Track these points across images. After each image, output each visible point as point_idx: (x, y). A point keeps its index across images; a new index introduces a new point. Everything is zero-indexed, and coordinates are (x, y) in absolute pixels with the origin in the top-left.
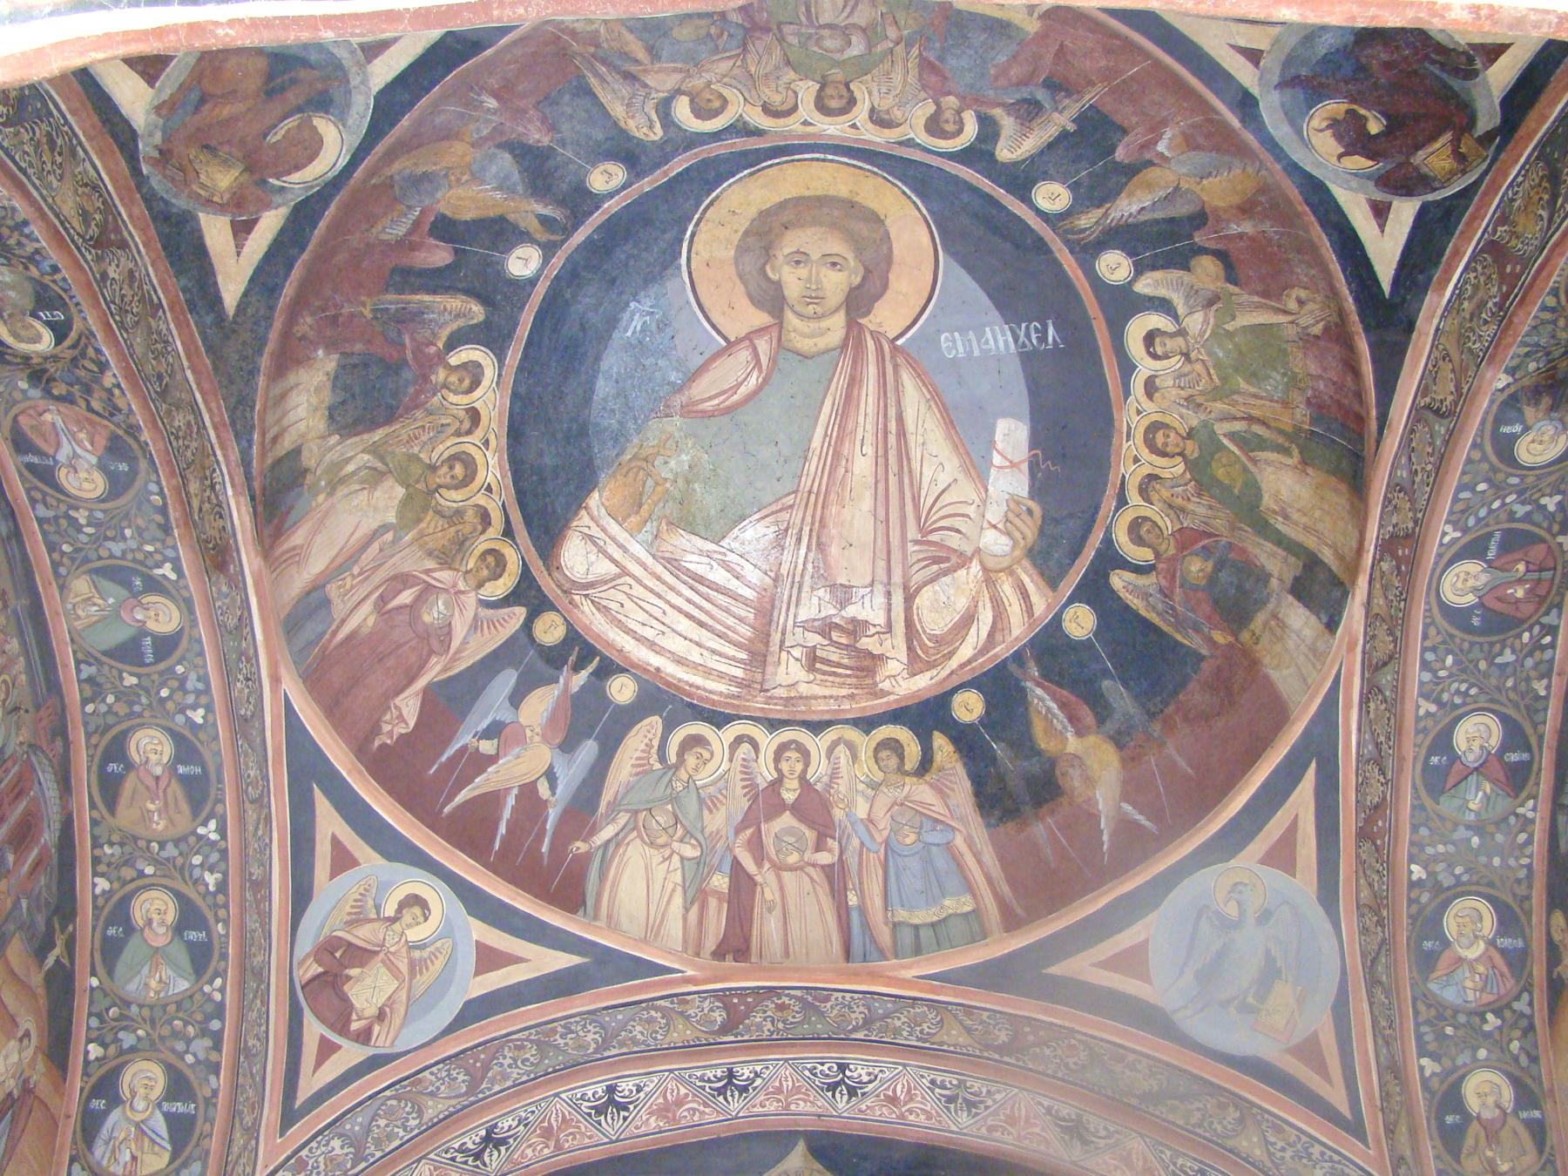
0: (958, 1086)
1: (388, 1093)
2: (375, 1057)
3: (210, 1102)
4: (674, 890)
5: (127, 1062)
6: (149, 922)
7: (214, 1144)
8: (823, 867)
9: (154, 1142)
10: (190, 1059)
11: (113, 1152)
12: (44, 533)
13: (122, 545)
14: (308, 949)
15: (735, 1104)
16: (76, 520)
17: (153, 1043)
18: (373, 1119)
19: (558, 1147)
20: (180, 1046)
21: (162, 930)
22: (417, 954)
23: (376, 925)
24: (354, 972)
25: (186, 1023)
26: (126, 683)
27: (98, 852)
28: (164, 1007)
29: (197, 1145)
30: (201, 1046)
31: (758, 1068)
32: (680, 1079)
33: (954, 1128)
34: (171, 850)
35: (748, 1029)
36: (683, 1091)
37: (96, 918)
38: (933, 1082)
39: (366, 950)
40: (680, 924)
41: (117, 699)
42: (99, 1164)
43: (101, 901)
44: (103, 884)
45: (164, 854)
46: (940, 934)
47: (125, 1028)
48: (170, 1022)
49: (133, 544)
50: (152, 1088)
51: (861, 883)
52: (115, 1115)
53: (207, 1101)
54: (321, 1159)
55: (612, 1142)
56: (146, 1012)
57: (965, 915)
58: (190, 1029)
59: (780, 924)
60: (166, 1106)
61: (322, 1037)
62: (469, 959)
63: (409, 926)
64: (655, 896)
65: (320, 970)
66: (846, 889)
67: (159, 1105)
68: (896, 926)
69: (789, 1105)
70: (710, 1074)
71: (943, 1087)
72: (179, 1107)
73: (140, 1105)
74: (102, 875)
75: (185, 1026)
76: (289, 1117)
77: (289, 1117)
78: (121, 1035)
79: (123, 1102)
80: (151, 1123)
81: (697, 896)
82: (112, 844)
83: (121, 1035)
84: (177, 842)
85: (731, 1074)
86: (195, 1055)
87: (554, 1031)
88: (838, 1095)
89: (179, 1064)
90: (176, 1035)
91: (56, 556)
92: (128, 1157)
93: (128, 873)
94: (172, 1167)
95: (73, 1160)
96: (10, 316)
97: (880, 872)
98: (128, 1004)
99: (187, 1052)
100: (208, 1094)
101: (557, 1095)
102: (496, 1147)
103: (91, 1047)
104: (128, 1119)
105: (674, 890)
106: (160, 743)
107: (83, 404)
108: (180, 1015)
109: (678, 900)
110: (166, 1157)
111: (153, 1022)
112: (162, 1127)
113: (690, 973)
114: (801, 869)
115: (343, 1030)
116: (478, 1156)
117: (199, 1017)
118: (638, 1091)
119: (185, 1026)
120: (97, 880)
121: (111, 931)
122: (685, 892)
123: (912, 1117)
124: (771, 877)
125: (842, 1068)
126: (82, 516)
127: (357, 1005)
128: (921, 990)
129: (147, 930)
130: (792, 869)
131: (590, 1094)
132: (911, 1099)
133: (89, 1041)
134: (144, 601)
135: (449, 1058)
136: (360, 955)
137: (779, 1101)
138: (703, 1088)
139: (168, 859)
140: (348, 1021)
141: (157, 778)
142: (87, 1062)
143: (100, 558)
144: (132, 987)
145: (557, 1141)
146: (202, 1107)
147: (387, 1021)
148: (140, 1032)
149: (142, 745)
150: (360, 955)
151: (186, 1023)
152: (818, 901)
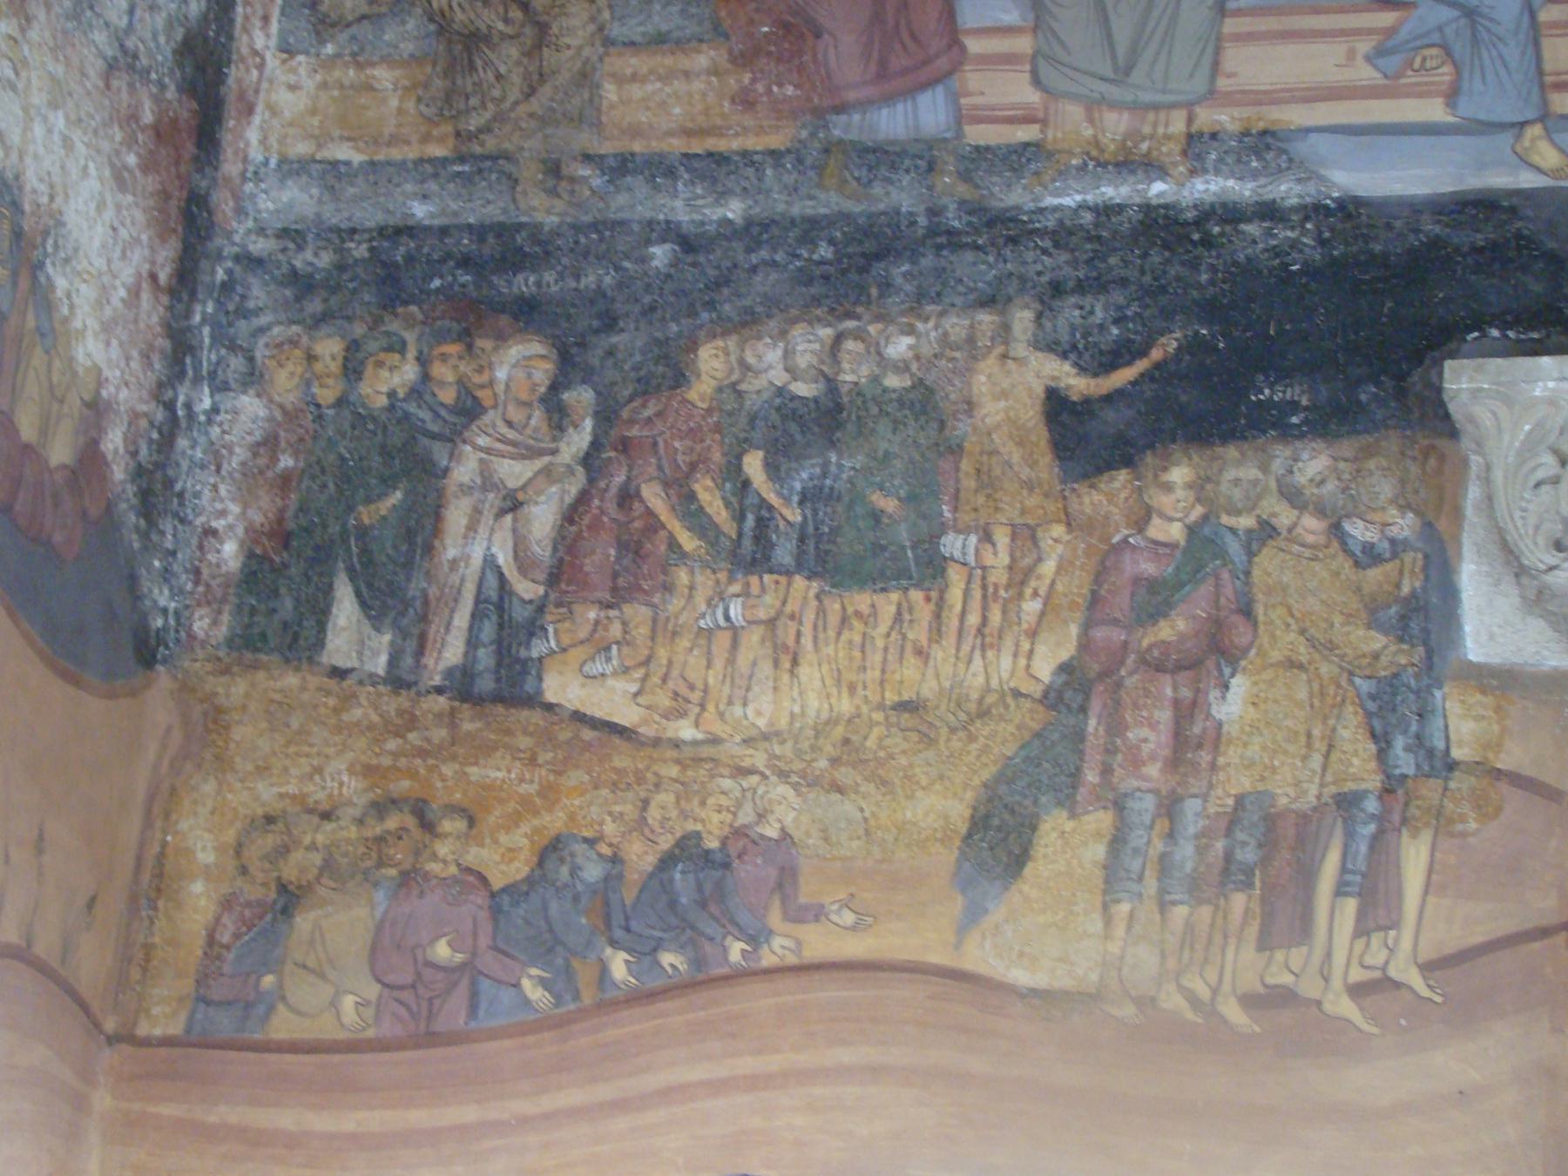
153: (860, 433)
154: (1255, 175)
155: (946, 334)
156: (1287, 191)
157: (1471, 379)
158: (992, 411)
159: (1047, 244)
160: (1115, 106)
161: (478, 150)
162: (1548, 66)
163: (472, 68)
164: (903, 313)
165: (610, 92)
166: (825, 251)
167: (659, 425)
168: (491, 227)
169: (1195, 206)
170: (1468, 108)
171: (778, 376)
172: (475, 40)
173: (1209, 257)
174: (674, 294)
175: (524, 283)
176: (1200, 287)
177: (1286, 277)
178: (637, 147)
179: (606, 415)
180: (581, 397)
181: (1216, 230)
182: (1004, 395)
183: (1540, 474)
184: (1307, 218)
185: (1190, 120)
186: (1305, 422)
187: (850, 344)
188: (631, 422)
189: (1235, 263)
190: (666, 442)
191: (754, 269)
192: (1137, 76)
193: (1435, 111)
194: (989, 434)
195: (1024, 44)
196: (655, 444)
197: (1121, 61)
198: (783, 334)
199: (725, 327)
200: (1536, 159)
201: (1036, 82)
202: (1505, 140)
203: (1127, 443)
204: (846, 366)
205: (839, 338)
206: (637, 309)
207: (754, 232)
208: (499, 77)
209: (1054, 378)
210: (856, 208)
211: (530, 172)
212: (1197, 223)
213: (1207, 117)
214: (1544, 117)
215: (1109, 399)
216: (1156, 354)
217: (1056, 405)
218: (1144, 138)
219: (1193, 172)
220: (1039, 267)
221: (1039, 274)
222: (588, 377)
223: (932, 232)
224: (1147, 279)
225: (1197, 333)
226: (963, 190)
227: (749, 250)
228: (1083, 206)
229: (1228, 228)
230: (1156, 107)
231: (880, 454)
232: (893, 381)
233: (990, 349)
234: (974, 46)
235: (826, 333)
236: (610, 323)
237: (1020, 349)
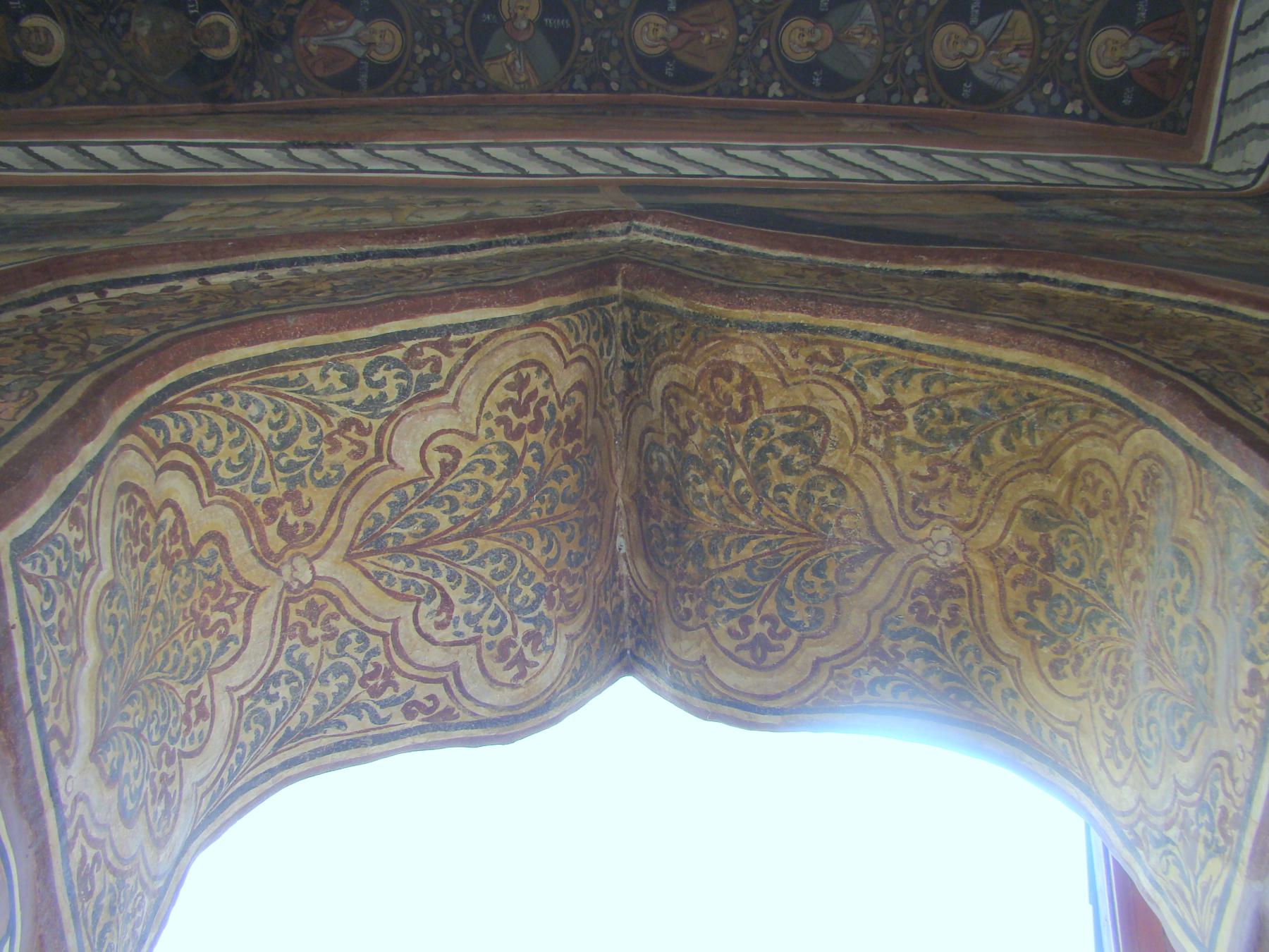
6: (810, 45)
9: (1004, 28)
11: (1009, 70)
12: (442, 92)
13: (450, 22)
16: (426, 58)
21: (818, 32)
26: (591, 49)
27: (745, 92)
34: (746, 22)
37: (804, 97)
41: (606, 60)
43: (790, 91)
44: (775, 89)
45: (750, 29)
47: (904, 66)
49: (447, 12)
50: (957, 37)
52: (979, 73)
56: (890, 48)
60: (974, 21)
67: (973, 27)
73: (971, 47)
74: (767, 89)
78: (909, 70)
79: (968, 65)
82: (739, 79)
83: (909, 70)
84: (739, 17)
91: (465, 87)
92: (1015, 55)
93: (765, 65)
95: (1012, 110)
96: (196, 38)
98: (882, 66)
103: (916, 100)
106: (647, 24)
107: (292, 12)
120: (770, 94)
121: (817, 81)
126: (421, 54)
129: (818, 48)
133: (911, 103)
134: (507, 16)
139: (754, 26)
141: (681, 31)
142: (930, 104)
143: (464, 46)
144: (867, 62)
148: (908, 53)
149: (649, 43)
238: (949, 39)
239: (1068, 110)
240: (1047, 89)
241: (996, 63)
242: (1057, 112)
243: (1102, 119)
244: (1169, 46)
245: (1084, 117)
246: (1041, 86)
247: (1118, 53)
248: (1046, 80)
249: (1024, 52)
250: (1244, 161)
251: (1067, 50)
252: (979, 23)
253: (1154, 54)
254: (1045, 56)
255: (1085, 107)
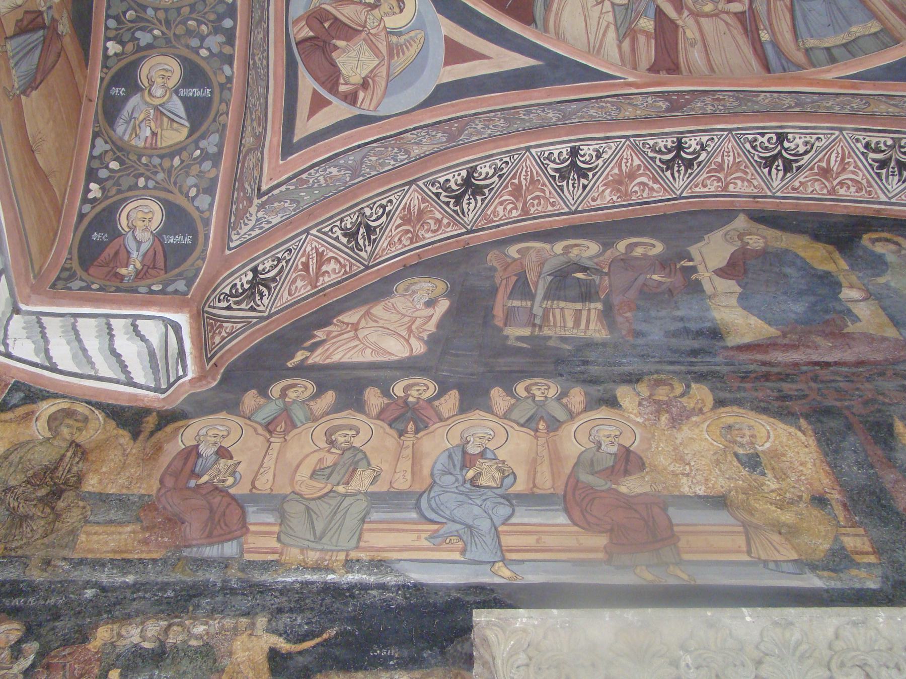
0: (892, 147)
1: (374, 145)
2: (360, 116)
3: (225, 86)
4: (607, 27)
5: (144, 57)
7: (230, 120)
8: (735, 14)
9: (173, 120)
10: (204, 53)
11: (134, 128)
14: (301, 12)
15: (680, 182)
17: (168, 41)
18: (364, 157)
19: (525, 211)
20: (195, 43)
22: (394, 39)
23: (359, 8)
24: (341, 43)
25: (200, 23)
28: (179, 10)
29: (214, 120)
30: (215, 42)
31: (704, 139)
32: (635, 148)
33: (883, 198)
35: (693, 110)
36: (637, 162)
38: (867, 146)
39: (350, 27)
40: (616, 51)
42: (121, 139)
46: (851, 48)
47: (142, 29)
48: (184, 22)
50: (169, 78)
51: (771, 24)
53: (222, 87)
54: (321, 178)
55: (571, 213)
56: (161, 15)
57: (875, 34)
58: (204, 27)
59: (703, 55)
60: (182, 92)
61: (314, 90)
62: (439, 51)
63: (387, 14)
64: (593, 29)
65: (311, 34)
66: (757, 30)
67: (176, 92)
68: (808, 51)
69: (727, 185)
70: (661, 143)
71: (877, 150)
72: (195, 92)
73: (158, 92)
75: (199, 26)
76: (288, 148)
77: (288, 148)
78: (138, 34)
79: (142, 90)
80: (169, 106)
81: (628, 32)
83: (138, 34)
85: (680, 146)
86: (209, 49)
87: (518, 113)
88: (774, 171)
89: (193, 57)
90: (190, 33)
92: (148, 133)
94: (190, 140)
95: (96, 135)
97: (788, 16)
98: (144, 8)
99: (201, 47)
100: (223, 80)
101: (528, 149)
102: (474, 194)
103: (110, 44)
104: (146, 103)
105: (607, 27)
108: (194, 16)
109: (612, 34)
110: (185, 132)
111: (168, 23)
112: (179, 108)
113: (631, 79)
114: (716, 15)
115: (333, 90)
116: (458, 199)
117: (212, 17)
118: (598, 157)
119: (199, 26)
122: (617, 29)
123: (842, 191)
124: (690, 21)
125: (781, 138)
127: (344, 71)
128: (841, 87)
130: (707, 15)
131: (556, 153)
132: (844, 169)
133: (108, 39)
135: (426, 126)
136: (348, 32)
137: (719, 180)
138: (652, 159)
140: (336, 84)
142: (106, 57)
145: (525, 203)
146: (217, 90)
147: (370, 91)
148: (156, 32)
150: (348, 32)
151: (200, 23)
152: (734, 38)
153: (172, 663)
154: (376, 574)
155: (223, 625)
156: (390, 579)
157: (486, 617)
158: (241, 655)
159: (277, 594)
160: (313, 549)
161: (13, 554)
162: (503, 544)
163: (21, 526)
164: (204, 617)
165: (83, 537)
166: (170, 593)
167: (69, 658)
168: (9, 582)
169: (348, 584)
170: (469, 556)
171: (136, 640)
172: (26, 518)
173: (354, 602)
174: (93, 608)
175: (17, 602)
176: (348, 612)
177: (388, 609)
178: (90, 556)
179: (42, 654)
180: (32, 648)
181: (357, 592)
182: (248, 649)
183: (519, 662)
184: (399, 589)
185: (347, 556)
186: (397, 663)
187: (175, 628)
188: (55, 657)
189: (365, 604)
190: (70, 665)
191: (134, 600)
192: (323, 541)
193: (457, 556)
194: (239, 665)
195: (276, 529)
196: (65, 666)
197: (318, 533)
198: (142, 623)
199: (113, 620)
200: (501, 574)
201: (279, 540)
202: (488, 567)
203: (308, 670)
204: (171, 636)
205: (170, 626)
206: (72, 612)
207: (135, 587)
208: (32, 530)
209: (274, 644)
210: (188, 579)
211: (35, 562)
212: (348, 590)
213: (354, 555)
214: (503, 560)
215: (300, 653)
216: (325, 636)
217: (274, 655)
218: (326, 560)
219: (347, 572)
220: (272, 602)
221: (272, 605)
222: (38, 638)
223: (223, 589)
224: (323, 608)
225: (345, 629)
226: (240, 574)
227: (133, 593)
228: (296, 581)
229: (362, 592)
230: (332, 551)
231: (181, 672)
232: (193, 643)
233: (244, 632)
234: (252, 528)
235: (164, 623)
236: (57, 617)
237: (259, 632)
238: (167, 71)
239: (93, 186)
240: (114, 165)
241: (142, 117)
242: (92, 176)
243: (81, 216)
244: (139, 266)
245: (85, 200)
246: (117, 159)
247: (139, 224)
248: (122, 163)
249: (149, 140)
250: (15, 340)
251: (147, 179)
252: (181, 98)
253: (134, 255)
254: (144, 160)
255: (95, 199)
